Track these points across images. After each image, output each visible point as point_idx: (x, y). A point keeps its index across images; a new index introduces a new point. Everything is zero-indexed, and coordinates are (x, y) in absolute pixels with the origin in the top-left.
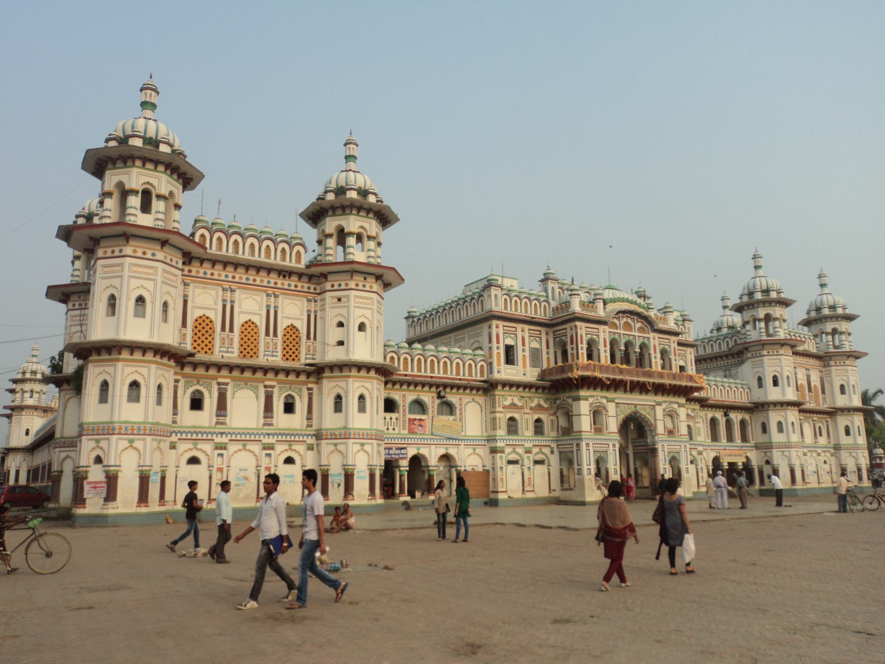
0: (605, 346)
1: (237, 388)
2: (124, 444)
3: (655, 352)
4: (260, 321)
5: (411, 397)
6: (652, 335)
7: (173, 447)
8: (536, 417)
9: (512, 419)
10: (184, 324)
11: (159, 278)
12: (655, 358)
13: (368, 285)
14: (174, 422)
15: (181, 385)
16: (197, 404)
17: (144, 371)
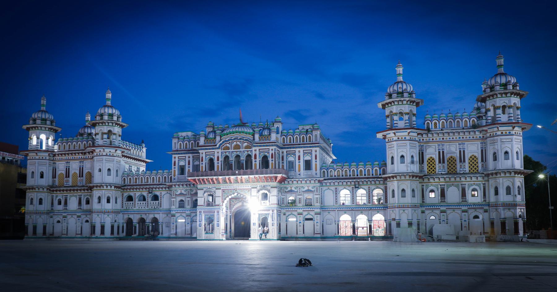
0: (218, 160)
1: (71, 196)
2: (29, 217)
3: (255, 158)
4: (78, 172)
5: (138, 194)
6: (254, 149)
7: (51, 217)
8: (194, 199)
9: (182, 201)
10: (55, 177)
11: (37, 165)
12: (255, 161)
13: (101, 153)
14: (52, 209)
15: (54, 197)
16: (60, 203)
17: (33, 195)
